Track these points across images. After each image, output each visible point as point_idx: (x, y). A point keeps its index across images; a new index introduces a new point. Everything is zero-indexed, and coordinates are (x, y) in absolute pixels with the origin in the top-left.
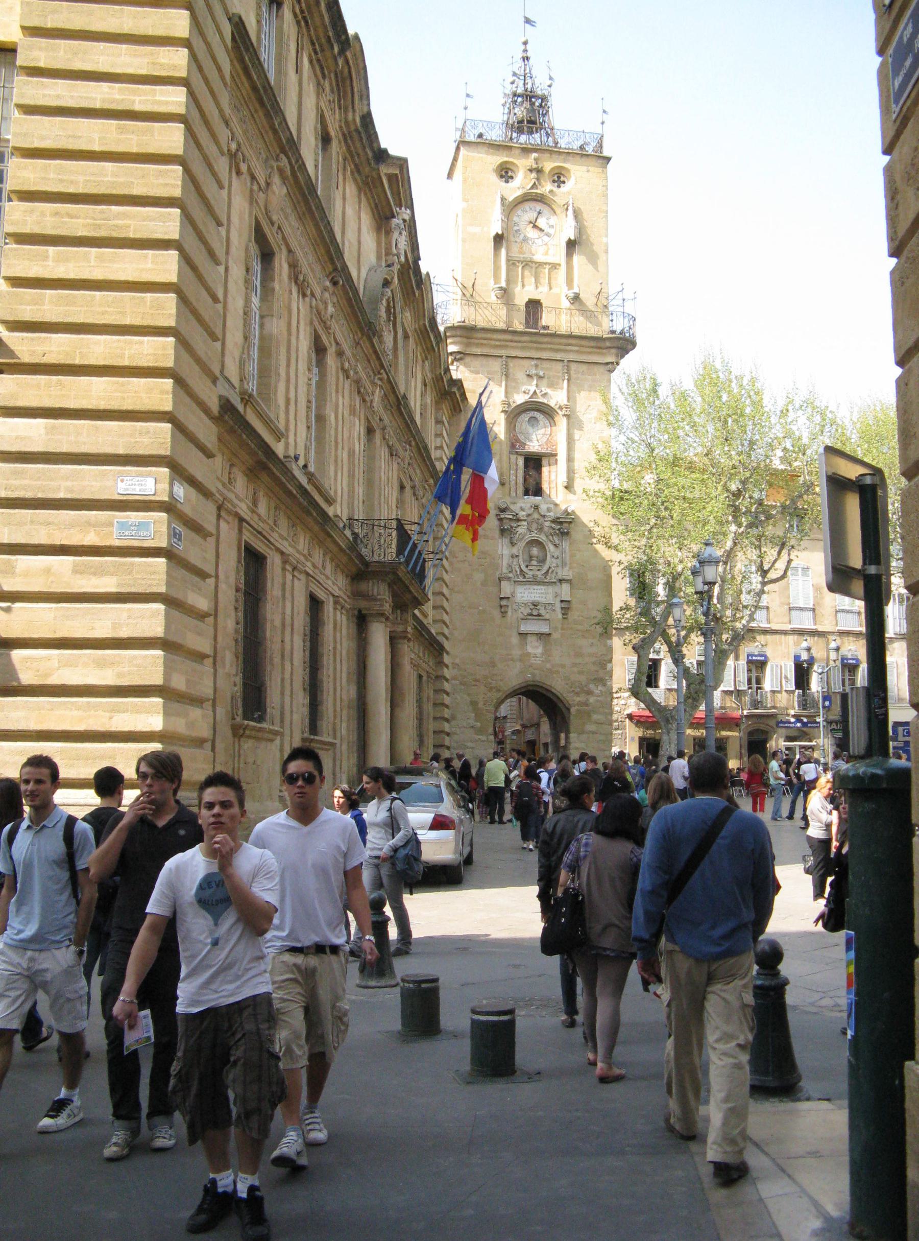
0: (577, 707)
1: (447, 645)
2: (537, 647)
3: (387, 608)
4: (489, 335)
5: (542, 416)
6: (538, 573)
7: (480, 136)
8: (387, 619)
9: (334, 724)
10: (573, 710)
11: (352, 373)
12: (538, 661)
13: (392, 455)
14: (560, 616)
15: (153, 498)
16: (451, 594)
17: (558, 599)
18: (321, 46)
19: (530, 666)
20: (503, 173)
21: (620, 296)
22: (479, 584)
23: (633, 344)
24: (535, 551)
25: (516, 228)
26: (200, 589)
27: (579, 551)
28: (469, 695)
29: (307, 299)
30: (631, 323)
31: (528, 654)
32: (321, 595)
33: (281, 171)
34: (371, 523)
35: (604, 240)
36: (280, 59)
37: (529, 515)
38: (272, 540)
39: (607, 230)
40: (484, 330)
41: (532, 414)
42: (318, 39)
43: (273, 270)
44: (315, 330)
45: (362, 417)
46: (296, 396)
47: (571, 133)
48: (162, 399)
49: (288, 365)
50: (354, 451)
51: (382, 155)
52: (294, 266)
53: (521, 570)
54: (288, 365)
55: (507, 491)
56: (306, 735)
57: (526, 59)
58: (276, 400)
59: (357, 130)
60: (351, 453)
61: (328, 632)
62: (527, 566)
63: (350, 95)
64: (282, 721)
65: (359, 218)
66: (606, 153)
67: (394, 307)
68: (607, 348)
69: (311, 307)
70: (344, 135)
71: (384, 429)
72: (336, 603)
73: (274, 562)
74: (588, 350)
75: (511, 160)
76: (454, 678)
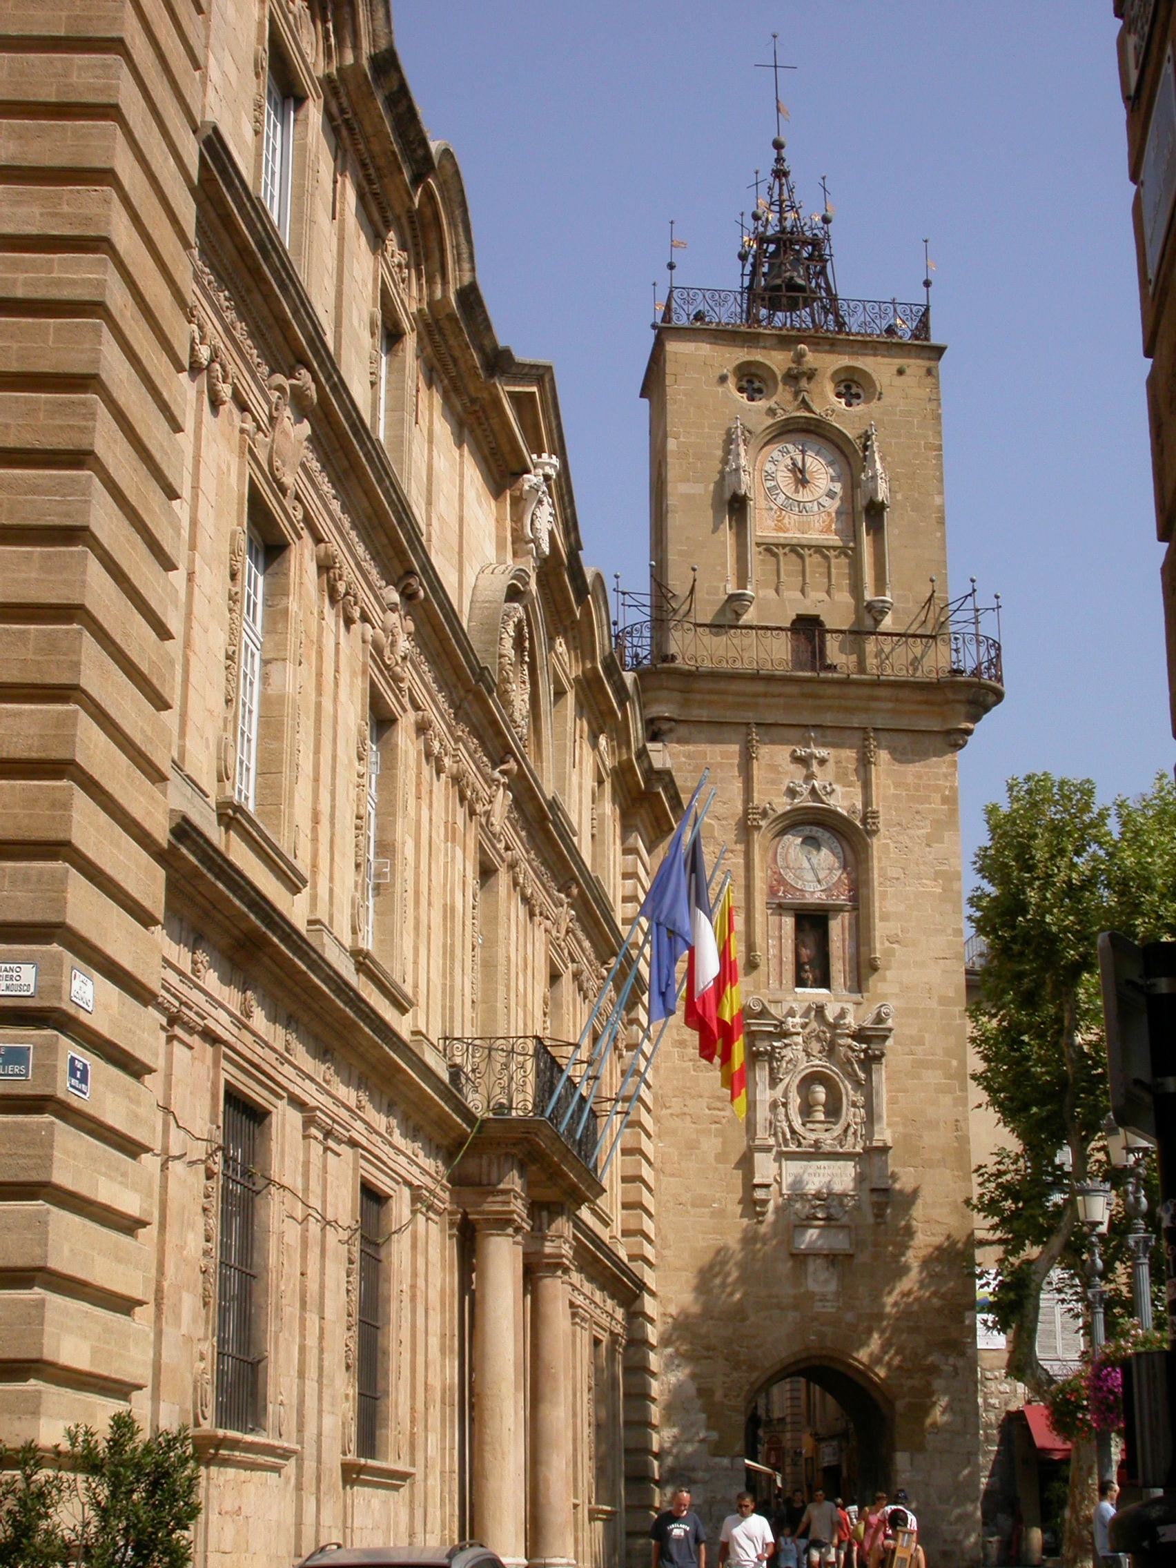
0: (907, 1400)
1: (650, 1278)
2: (827, 1281)
3: (518, 1207)
4: (723, 685)
5: (827, 835)
6: (827, 1135)
7: (699, 317)
8: (518, 1230)
9: (412, 1434)
10: (900, 1405)
11: (447, 761)
12: (830, 1308)
13: (532, 915)
14: (870, 1220)
15: (30, 1003)
16: (657, 1180)
17: (867, 1186)
18: (378, 169)
19: (814, 1319)
20: (744, 384)
21: (969, 603)
22: (711, 1159)
23: (999, 696)
24: (820, 1093)
25: (769, 484)
26: (125, 1174)
27: (906, 1091)
29: (357, 627)
30: (993, 653)
31: (811, 1295)
32: (383, 1183)
33: (298, 397)
34: (488, 1045)
35: (938, 500)
36: (301, 195)
37: (804, 1026)
38: (280, 1079)
39: (941, 480)
40: (714, 675)
41: (808, 830)
42: (373, 157)
43: (287, 575)
44: (373, 685)
45: (471, 844)
46: (333, 807)
47: (868, 305)
48: (54, 818)
49: (317, 751)
50: (453, 909)
51: (500, 363)
52: (325, 566)
53: (793, 1132)
54: (317, 751)
55: (763, 979)
56: (351, 1457)
57: (780, 174)
58: (291, 815)
59: (451, 317)
60: (449, 912)
61: (399, 1253)
62: (804, 1125)
63: (437, 255)
64: (300, 1430)
65: (462, 476)
66: (935, 340)
67: (531, 639)
68: (947, 702)
69: (364, 641)
70: (427, 325)
71: (512, 866)
72: (416, 1198)
73: (285, 1121)
74: (914, 707)
75: (759, 358)
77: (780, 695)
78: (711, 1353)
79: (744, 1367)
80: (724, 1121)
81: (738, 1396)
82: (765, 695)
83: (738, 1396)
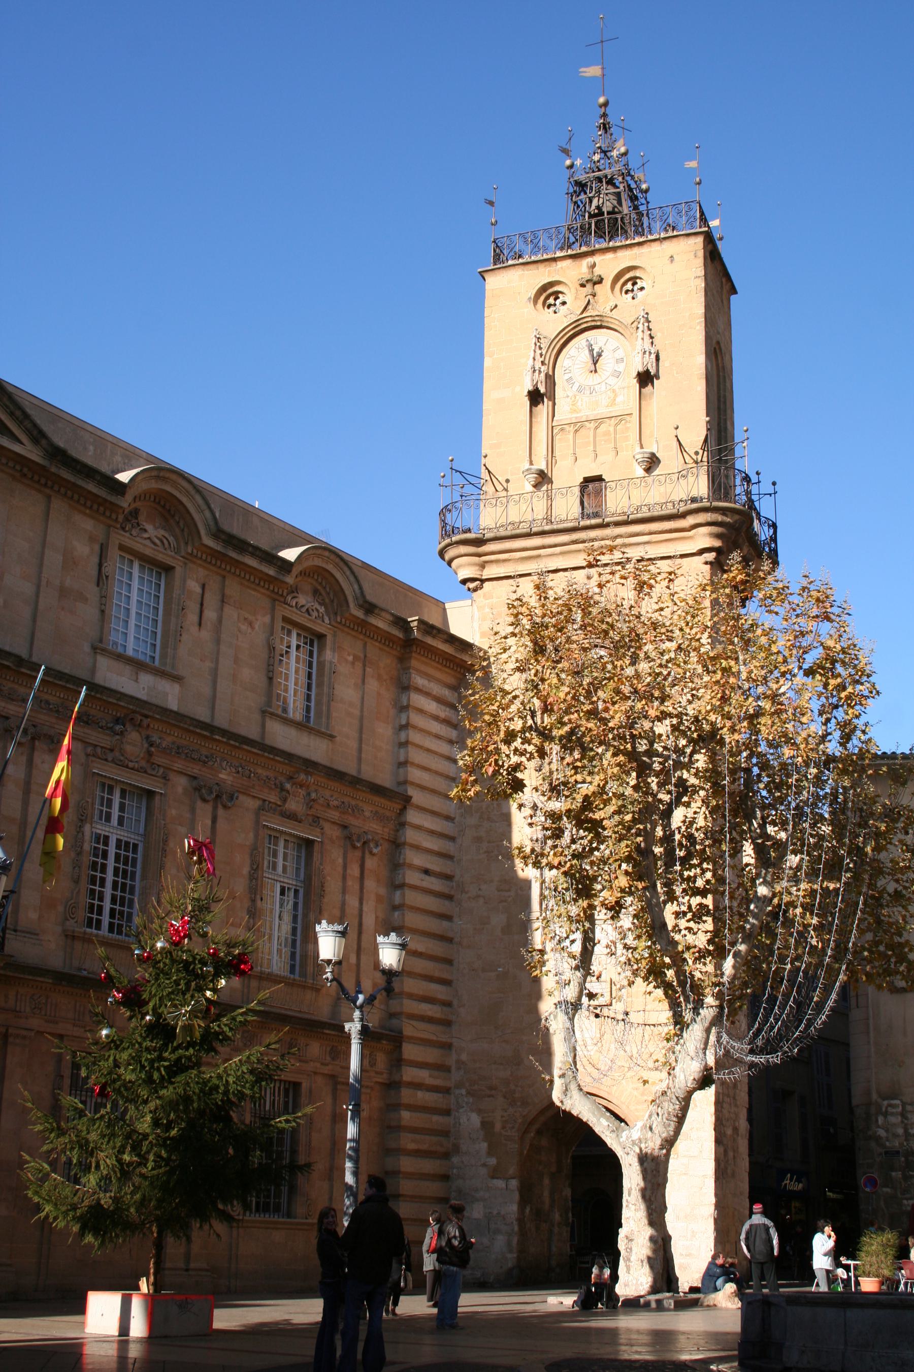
25: (567, 377)
28: (479, 1111)
76: (459, 1085)
77: (555, 546)
78: (493, 1092)
79: (519, 1104)
80: (509, 900)
81: (513, 1128)
82: (544, 547)
83: (513, 1128)
